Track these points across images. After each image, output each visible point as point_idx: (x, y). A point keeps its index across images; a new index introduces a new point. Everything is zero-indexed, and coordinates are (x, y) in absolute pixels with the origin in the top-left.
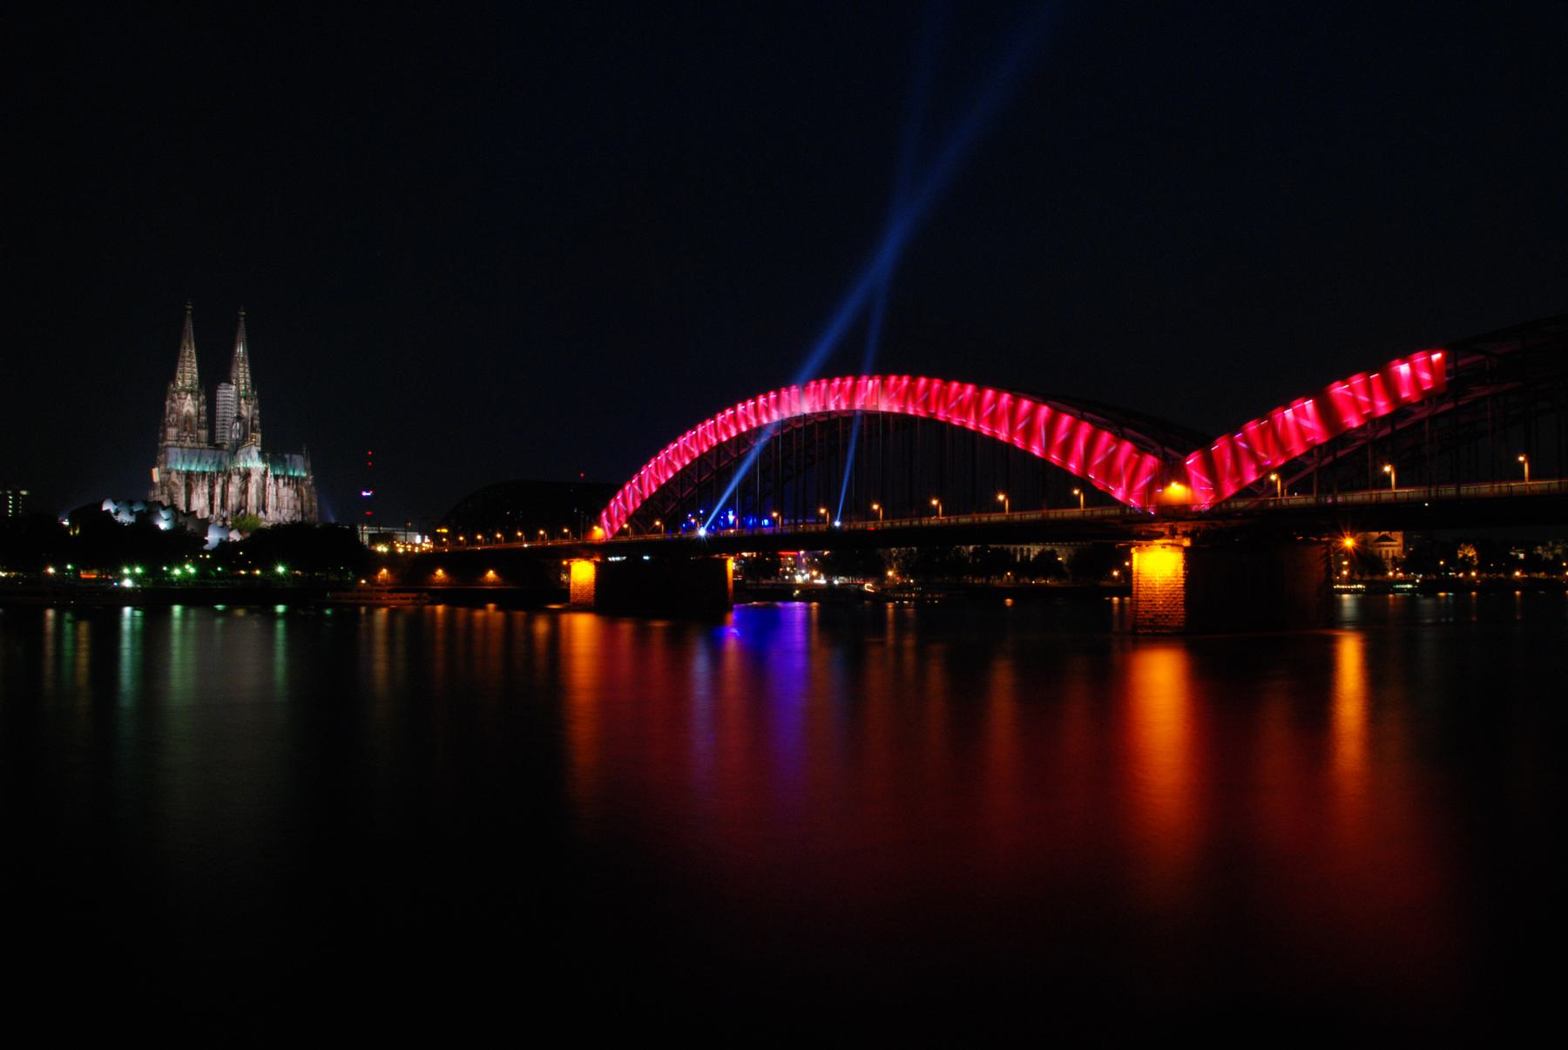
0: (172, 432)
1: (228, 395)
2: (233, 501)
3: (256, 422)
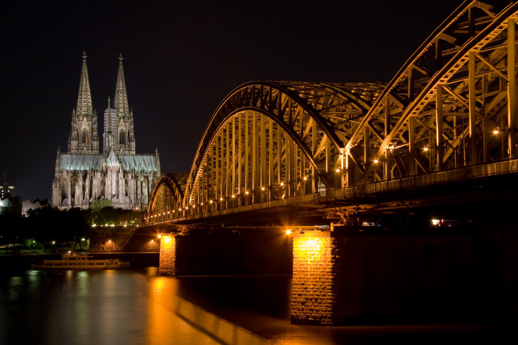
0: (74, 143)
1: (110, 115)
2: (96, 191)
3: (132, 134)
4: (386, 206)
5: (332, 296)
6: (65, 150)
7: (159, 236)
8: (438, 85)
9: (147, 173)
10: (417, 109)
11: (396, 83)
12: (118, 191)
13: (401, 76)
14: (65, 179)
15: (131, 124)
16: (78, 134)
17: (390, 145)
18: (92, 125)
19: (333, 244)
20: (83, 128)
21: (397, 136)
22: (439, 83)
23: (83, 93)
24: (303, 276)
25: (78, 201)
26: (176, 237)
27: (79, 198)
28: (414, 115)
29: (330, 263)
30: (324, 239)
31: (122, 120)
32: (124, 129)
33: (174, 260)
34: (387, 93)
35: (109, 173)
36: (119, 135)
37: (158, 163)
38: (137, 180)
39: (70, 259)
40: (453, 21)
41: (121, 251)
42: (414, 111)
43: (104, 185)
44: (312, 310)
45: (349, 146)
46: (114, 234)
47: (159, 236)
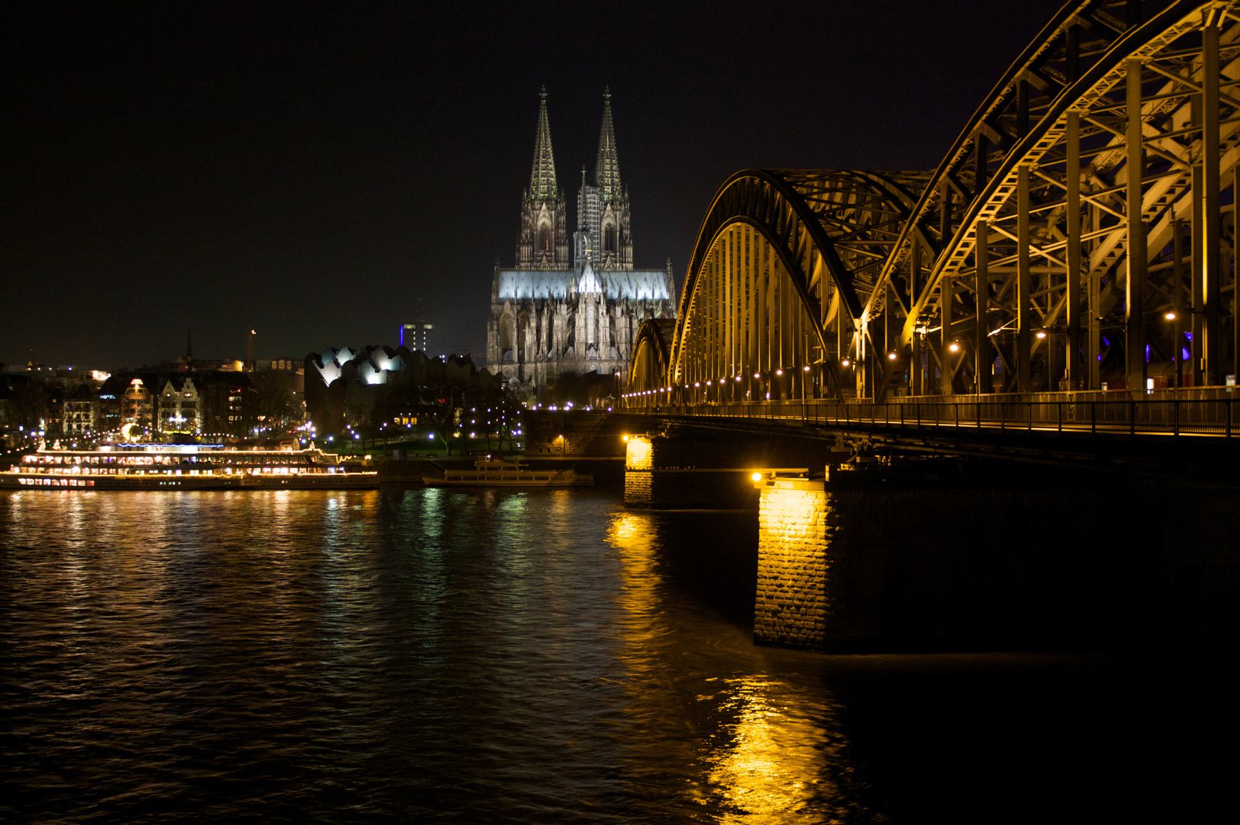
0: (525, 250)
1: (590, 199)
2: (559, 337)
3: (626, 232)
4: (911, 444)
5: (826, 601)
6: (511, 263)
7: (625, 438)
8: (980, 222)
9: (651, 304)
10: (953, 264)
11: (924, 207)
12: (597, 338)
13: (932, 195)
14: (508, 316)
15: (625, 215)
16: (532, 234)
17: (917, 326)
18: (557, 217)
19: (828, 504)
20: (540, 223)
21: (928, 310)
22: (978, 218)
23: (542, 159)
24: (776, 563)
25: (530, 355)
26: (653, 441)
27: (530, 349)
28: (948, 274)
29: (823, 541)
30: (814, 493)
31: (609, 207)
32: (612, 222)
33: (650, 482)
34: (913, 226)
35: (581, 306)
36: (603, 234)
37: (672, 285)
38: (631, 318)
39: (491, 469)
40: (997, 102)
41: (581, 455)
42: (947, 266)
43: (574, 327)
44: (790, 626)
45: (865, 317)
46: (566, 424)
47: (625, 438)
